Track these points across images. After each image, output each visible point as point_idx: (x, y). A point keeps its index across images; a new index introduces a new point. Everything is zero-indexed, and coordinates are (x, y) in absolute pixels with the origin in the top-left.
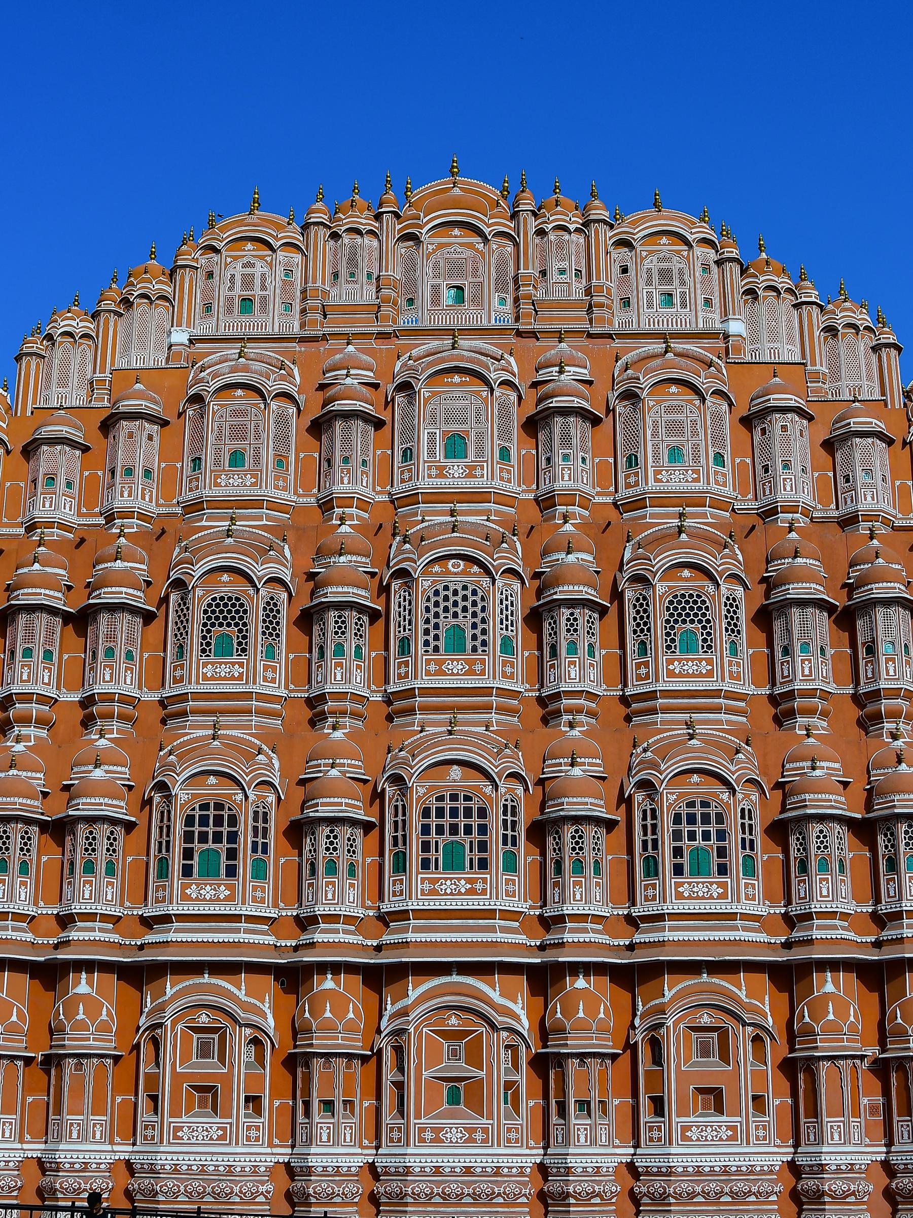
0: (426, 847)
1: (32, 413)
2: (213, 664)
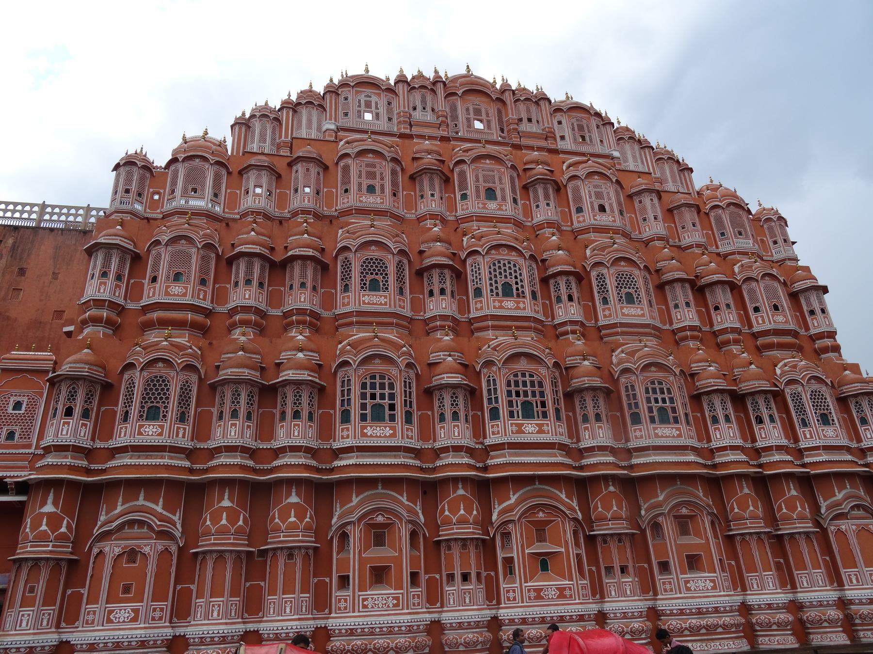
0: (510, 404)
1: (243, 155)
2: (368, 295)
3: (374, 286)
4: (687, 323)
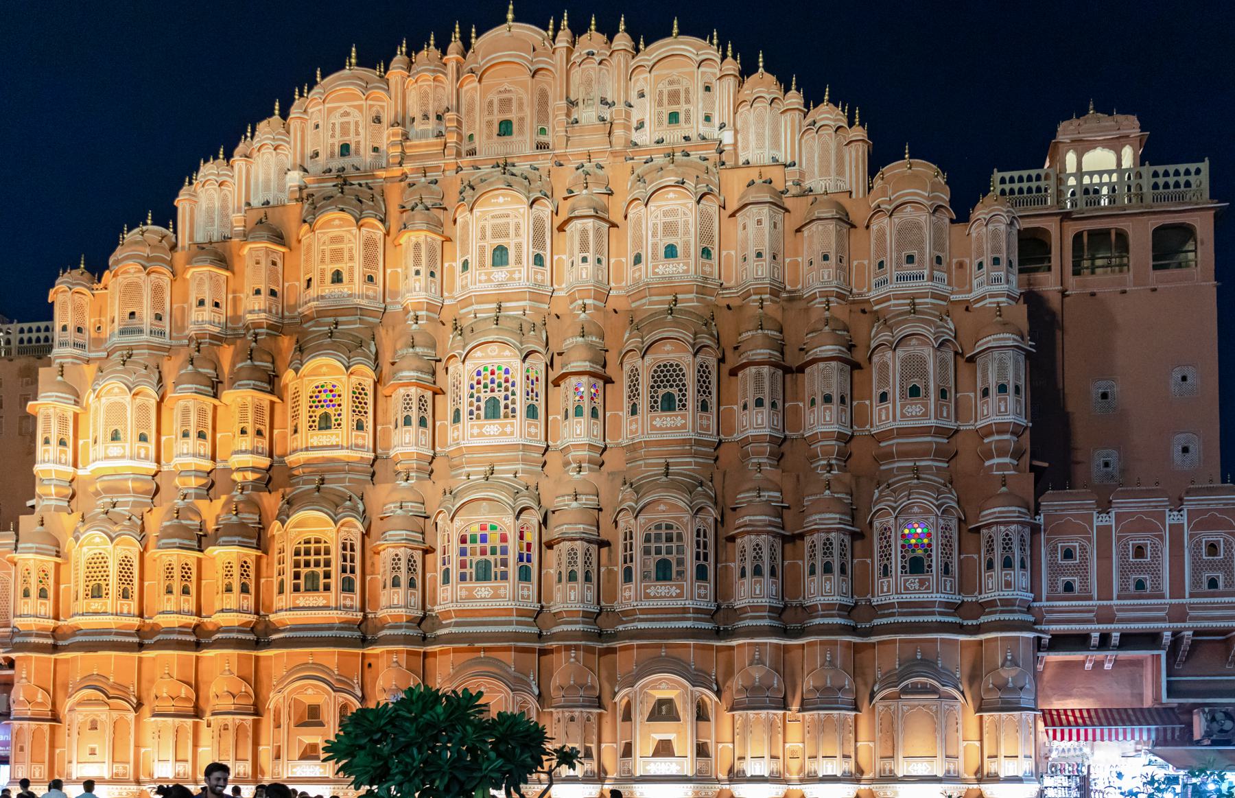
3: (325, 423)
4: (751, 432)
